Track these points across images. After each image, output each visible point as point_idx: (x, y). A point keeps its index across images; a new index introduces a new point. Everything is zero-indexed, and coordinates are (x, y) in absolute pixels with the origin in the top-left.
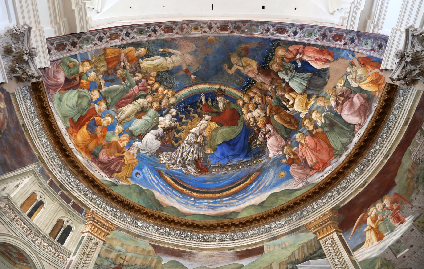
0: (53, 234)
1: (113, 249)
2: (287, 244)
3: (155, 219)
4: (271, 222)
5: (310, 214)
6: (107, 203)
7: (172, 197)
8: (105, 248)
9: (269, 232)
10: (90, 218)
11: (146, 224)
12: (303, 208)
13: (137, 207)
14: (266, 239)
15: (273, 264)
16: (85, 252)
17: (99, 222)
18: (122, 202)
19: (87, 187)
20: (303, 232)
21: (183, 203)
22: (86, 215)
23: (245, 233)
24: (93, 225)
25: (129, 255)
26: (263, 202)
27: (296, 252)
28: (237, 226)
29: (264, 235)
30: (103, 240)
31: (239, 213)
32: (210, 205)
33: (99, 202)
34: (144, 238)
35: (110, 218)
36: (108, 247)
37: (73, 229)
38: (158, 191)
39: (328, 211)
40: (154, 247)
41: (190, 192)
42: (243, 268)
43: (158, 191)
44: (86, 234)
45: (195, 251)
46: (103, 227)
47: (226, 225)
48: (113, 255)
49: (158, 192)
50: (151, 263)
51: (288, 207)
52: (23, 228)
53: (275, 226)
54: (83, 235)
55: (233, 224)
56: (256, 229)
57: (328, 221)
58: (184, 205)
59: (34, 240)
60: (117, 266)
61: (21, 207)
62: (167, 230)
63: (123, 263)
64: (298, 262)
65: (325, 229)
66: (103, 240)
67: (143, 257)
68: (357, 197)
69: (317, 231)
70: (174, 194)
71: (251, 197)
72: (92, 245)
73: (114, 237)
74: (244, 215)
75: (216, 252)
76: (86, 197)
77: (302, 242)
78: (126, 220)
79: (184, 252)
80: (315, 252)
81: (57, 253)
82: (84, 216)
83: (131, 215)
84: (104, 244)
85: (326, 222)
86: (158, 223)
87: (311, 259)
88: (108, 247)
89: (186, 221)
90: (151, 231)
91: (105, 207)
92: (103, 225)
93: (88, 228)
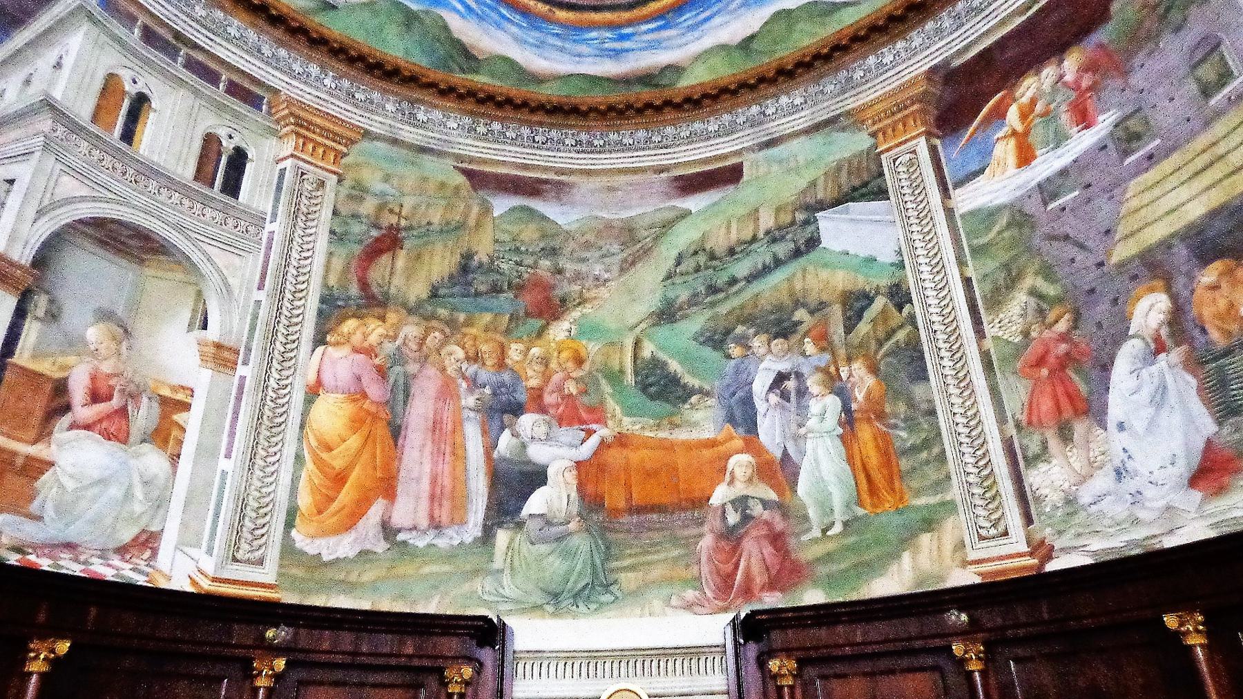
0: (203, 173)
1: (365, 190)
2: (801, 159)
3: (461, 97)
4: (767, 98)
5: (872, 80)
6: (322, 67)
7: (498, 26)
8: (344, 191)
9: (761, 123)
10: (284, 118)
11: (437, 115)
12: (854, 61)
13: (406, 69)
14: (750, 143)
15: (761, 210)
16: (298, 209)
17: (312, 124)
18: (361, 58)
19: (253, 25)
20: (843, 129)
21: (532, 45)
22: (273, 111)
23: (697, 126)
24: (298, 134)
25: (409, 202)
26: (752, 38)
27: (821, 183)
28: (678, 107)
29: (747, 132)
30: (335, 173)
31: (684, 69)
32: (606, 45)
33: (297, 68)
34: (440, 154)
35: (338, 108)
36: (353, 188)
37: (250, 156)
38: (458, 11)
39: (916, 77)
40: (469, 174)
41: (548, 7)
42: (689, 218)
43: (458, 11)
44: (288, 163)
45: (572, 179)
46: (327, 138)
47: (649, 105)
48: (368, 207)
49: (457, 17)
50: (466, 215)
51: (817, 57)
52: (124, 174)
53: (777, 110)
54: (281, 165)
55: (668, 103)
56: (726, 118)
57: (913, 104)
58: (534, 49)
59: (162, 198)
60: (384, 232)
61: (95, 118)
62: (496, 126)
63: (398, 224)
64: (822, 206)
65: (900, 126)
66: (335, 173)
67: (443, 203)
68: (1002, 44)
69: (879, 130)
70: (503, 17)
71: (717, 20)
72: (310, 188)
73: (361, 159)
74: (696, 78)
75: (623, 179)
76: (256, 58)
77: (838, 157)
78: (384, 108)
79: (546, 182)
80: (865, 184)
81: (231, 222)
82: (269, 113)
83: (396, 94)
84: (339, 181)
85: (906, 107)
86: (469, 107)
87: (853, 200)
88: (353, 188)
89: (543, 99)
90: (455, 132)
91: (317, 79)
92: (326, 133)
93: (290, 144)
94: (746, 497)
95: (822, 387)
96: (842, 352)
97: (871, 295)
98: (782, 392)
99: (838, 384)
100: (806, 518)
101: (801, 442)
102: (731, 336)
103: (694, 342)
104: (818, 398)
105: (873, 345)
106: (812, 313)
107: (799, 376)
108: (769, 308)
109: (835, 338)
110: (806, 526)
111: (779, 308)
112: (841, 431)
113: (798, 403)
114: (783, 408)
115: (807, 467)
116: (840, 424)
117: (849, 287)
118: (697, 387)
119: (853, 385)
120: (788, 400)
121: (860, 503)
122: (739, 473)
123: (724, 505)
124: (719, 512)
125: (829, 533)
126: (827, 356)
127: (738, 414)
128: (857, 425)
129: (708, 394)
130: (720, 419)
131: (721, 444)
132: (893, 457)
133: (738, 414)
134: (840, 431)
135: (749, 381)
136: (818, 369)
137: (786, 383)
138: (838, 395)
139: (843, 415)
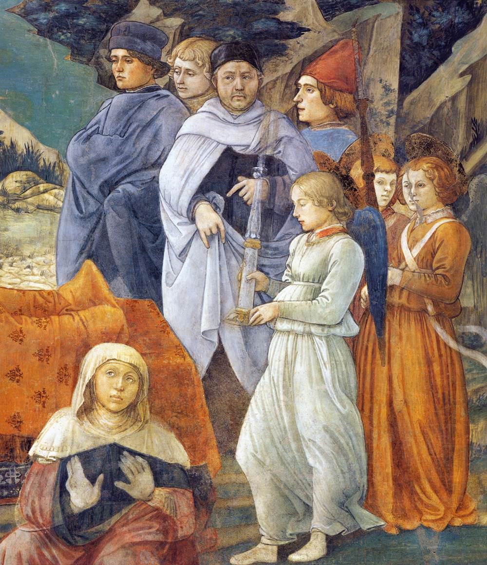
94: (117, 450)
95: (324, 214)
98: (229, 201)
99: (364, 212)
100: (248, 515)
101: (261, 334)
102: (122, 24)
103: (27, 25)
104: (314, 238)
105: (460, 137)
109: (376, 91)
110: (249, 533)
112: (355, 329)
113: (265, 237)
114: (227, 241)
115: (268, 401)
116: (353, 309)
118: (21, 147)
120: (242, 229)
121: (369, 500)
122: (107, 388)
123: (64, 461)
124: (52, 477)
125: (294, 557)
128: (393, 323)
129: (48, 175)
130: (75, 249)
131: (69, 311)
132: (460, 412)
134: (355, 329)
135: (154, 156)
137: (243, 181)
138: (357, 238)
139: (365, 290)
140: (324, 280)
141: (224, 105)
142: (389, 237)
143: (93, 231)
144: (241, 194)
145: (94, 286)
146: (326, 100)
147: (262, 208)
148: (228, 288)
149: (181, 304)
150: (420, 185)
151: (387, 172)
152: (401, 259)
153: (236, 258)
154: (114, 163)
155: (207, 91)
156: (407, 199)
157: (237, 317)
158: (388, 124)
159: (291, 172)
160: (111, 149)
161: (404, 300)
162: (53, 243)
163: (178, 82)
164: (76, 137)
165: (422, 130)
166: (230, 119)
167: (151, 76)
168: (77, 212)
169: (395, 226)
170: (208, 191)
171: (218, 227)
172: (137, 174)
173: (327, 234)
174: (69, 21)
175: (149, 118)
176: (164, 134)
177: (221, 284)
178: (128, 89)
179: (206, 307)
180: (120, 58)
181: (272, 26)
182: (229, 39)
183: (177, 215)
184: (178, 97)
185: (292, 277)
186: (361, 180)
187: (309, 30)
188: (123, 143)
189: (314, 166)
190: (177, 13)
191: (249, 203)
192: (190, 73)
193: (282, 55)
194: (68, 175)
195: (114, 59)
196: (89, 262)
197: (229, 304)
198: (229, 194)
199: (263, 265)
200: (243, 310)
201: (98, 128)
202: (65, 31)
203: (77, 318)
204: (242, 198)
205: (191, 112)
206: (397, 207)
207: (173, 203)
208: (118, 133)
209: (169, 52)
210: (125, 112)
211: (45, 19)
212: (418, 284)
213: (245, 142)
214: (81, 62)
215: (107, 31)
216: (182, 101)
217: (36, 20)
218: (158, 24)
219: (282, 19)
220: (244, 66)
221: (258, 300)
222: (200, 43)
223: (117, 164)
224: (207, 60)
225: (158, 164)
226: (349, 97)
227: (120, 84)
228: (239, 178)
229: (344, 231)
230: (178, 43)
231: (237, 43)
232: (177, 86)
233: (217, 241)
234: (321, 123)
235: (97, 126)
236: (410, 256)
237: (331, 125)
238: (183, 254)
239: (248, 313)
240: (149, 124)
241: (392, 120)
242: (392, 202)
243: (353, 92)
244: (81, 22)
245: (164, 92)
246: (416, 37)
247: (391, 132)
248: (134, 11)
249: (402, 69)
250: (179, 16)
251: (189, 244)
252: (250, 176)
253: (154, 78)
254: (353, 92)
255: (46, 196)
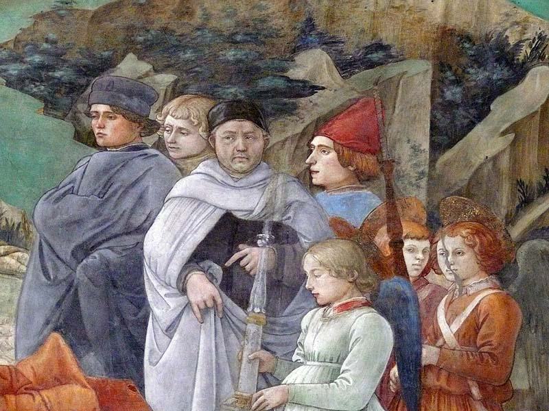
95: (343, 285)
96: (417, 196)
97: (521, 57)
98: (228, 272)
99: (392, 283)
102: (105, 78)
104: (331, 312)
105: (505, 198)
106: (346, 67)
107: (283, 235)
108: (227, 24)
109: (403, 152)
111: (255, 33)
114: (225, 317)
116: (381, 392)
117: (461, 20)
119: (438, 292)
120: (244, 303)
126: (369, 201)
127: (92, 311)
130: (39, 319)
131: (30, 389)
133: (92, 311)
135: (138, 220)
136: (341, 229)
137: (245, 249)
138: (384, 312)
139: (395, 371)
140: (344, 359)
141: (223, 167)
142: (423, 310)
143: (64, 297)
144: (242, 263)
145: (62, 363)
146: (344, 162)
147: (268, 279)
148: (227, 371)
149: (167, 387)
150: (457, 253)
151: (419, 239)
152: (437, 335)
153: (235, 333)
154: (90, 226)
155: (203, 151)
156: (444, 268)
157: (236, 402)
158: (418, 187)
159: (303, 240)
160: (86, 211)
161: (442, 383)
162: (13, 312)
163: (169, 140)
164: (45, 196)
165: (459, 193)
166: (231, 182)
167: (137, 134)
168: (44, 279)
169: (430, 298)
170: (203, 259)
171: (214, 301)
172: (118, 239)
173: (347, 307)
174: (43, 74)
175: (134, 179)
176: (151, 196)
177: (217, 363)
178: (109, 148)
179: (197, 390)
180: (102, 114)
181: (280, 83)
182: (230, 97)
183: (164, 285)
184: (169, 157)
185: (304, 356)
186: (387, 247)
187: (323, 88)
188: (102, 205)
189: (331, 232)
190: (170, 69)
191: (252, 273)
192: (183, 131)
193: (292, 114)
194: (35, 237)
195: (94, 114)
196: (56, 335)
197: (227, 386)
198: (228, 264)
199: (268, 343)
200: (244, 394)
201: (73, 187)
202: (38, 84)
203: (38, 398)
204: (243, 268)
205: (184, 173)
206: (432, 277)
207: (160, 271)
208: (97, 193)
209: (160, 110)
210: (106, 171)
211: (15, 70)
212: (458, 361)
213: (248, 206)
214: (56, 117)
215: (87, 86)
216: (172, 161)
217: (5, 71)
218: (146, 80)
219: (292, 77)
220: (248, 126)
221: (264, 384)
222: (195, 101)
223: (94, 227)
224: (204, 119)
225: (142, 230)
226: (371, 159)
227: (100, 142)
228: (241, 246)
229: (367, 304)
230: (170, 101)
231: (239, 101)
232: (168, 145)
233: (212, 315)
234: (338, 187)
235: (72, 185)
236: (448, 330)
237: (351, 188)
238: (170, 330)
239: (251, 398)
240: (133, 185)
241: (424, 183)
242: (425, 272)
243: (375, 152)
244: (58, 74)
245: (153, 151)
246: (448, 95)
247: (422, 195)
248: (119, 66)
249: (433, 127)
250: (171, 72)
251: (179, 317)
252: (254, 244)
253: (141, 136)
254: (375, 152)
255: (7, 259)
